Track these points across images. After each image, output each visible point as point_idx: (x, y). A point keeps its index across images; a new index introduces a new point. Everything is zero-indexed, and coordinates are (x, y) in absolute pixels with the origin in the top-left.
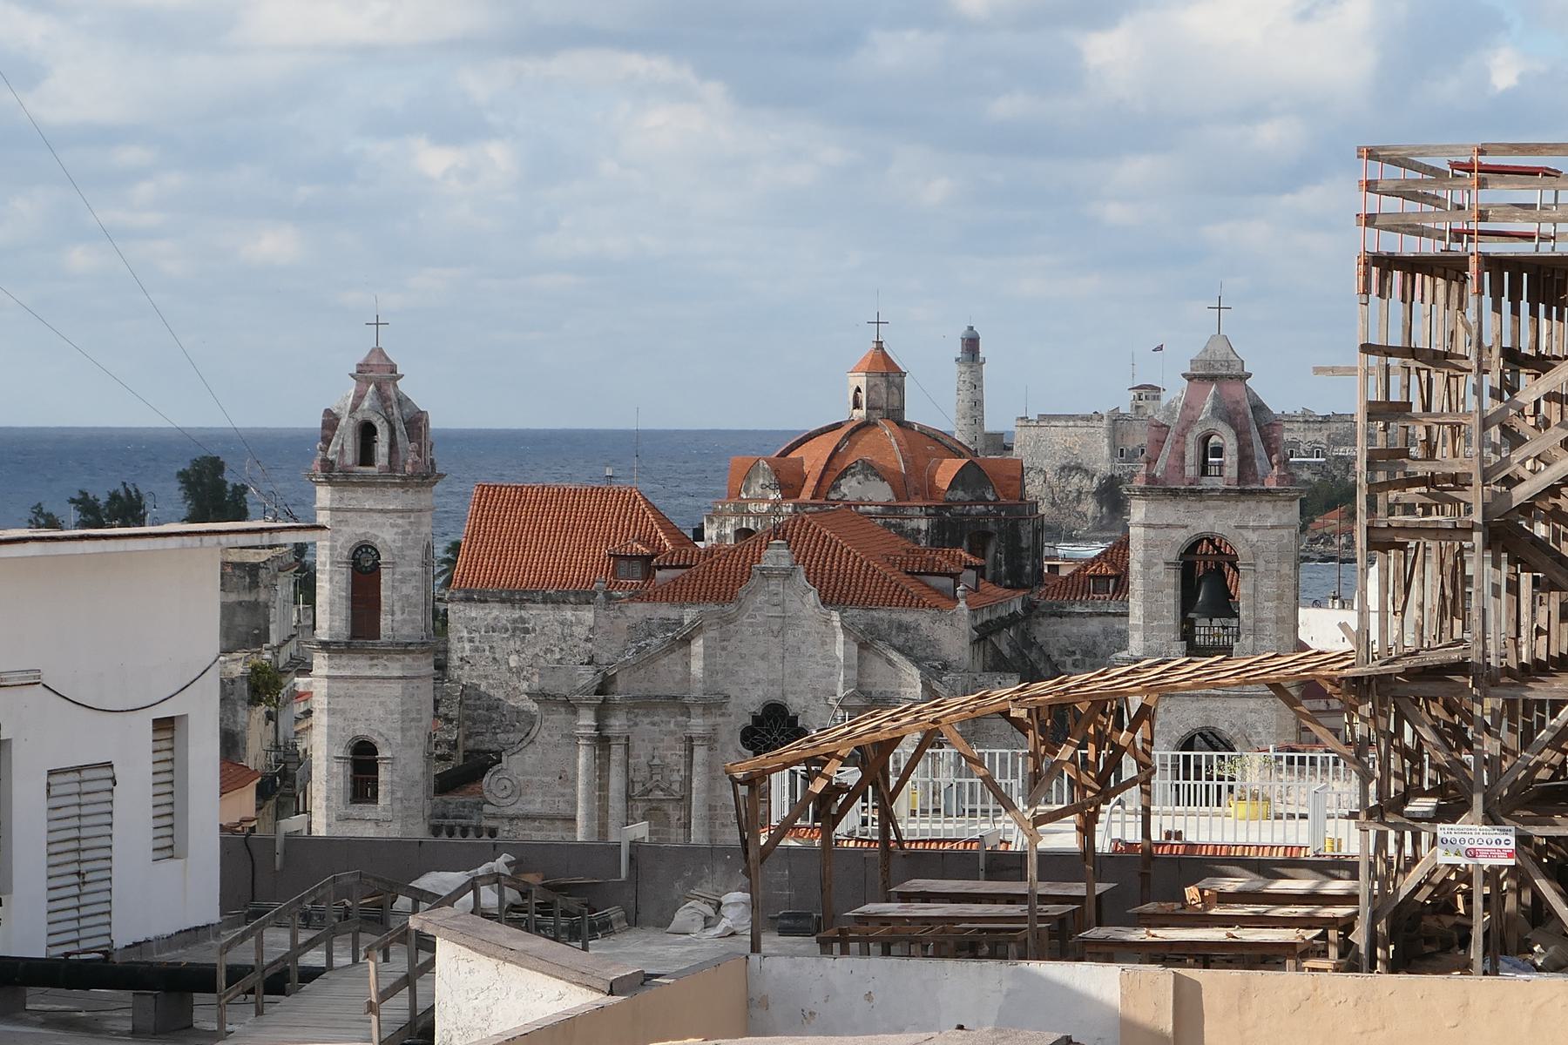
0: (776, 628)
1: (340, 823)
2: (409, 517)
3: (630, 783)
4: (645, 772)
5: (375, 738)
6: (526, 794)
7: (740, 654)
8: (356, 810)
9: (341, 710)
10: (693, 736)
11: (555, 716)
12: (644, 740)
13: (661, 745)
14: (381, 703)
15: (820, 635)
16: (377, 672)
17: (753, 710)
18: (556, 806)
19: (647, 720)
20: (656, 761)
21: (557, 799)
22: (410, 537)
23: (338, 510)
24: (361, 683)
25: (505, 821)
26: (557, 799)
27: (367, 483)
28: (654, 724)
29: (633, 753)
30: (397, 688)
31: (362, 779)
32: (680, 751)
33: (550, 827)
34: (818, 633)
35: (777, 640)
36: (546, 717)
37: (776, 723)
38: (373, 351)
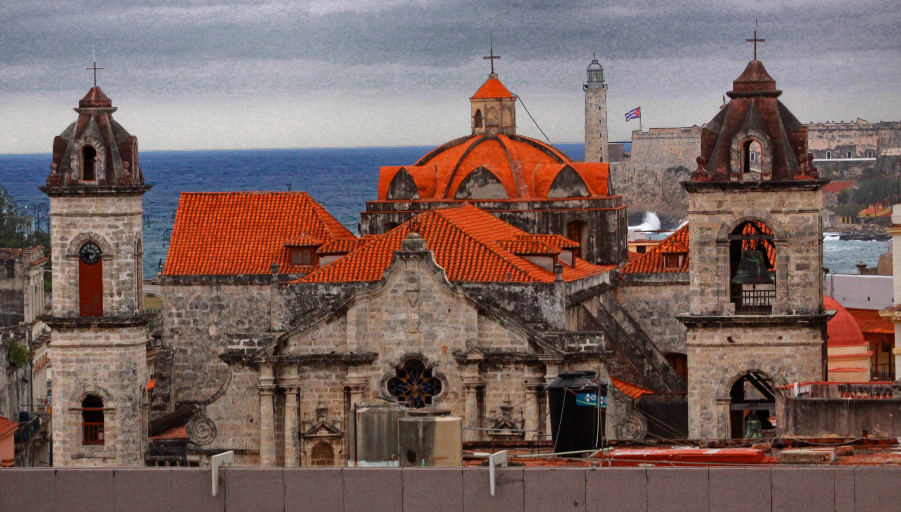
0: (413, 300)
1: (75, 461)
2: (123, 220)
3: (301, 424)
4: (312, 416)
5: (101, 393)
8: (85, 450)
9: (73, 372)
10: (350, 386)
11: (242, 373)
12: (311, 390)
13: (326, 393)
14: (106, 367)
16: (102, 341)
19: (312, 375)
20: (322, 406)
21: (245, 439)
22: (124, 236)
23: (68, 215)
24: (89, 350)
25: (204, 457)
26: (245, 439)
27: (90, 192)
28: (319, 377)
29: (304, 400)
30: (115, 352)
31: (91, 426)
32: (340, 397)
33: (239, 460)
34: (446, 303)
35: (414, 309)
36: (235, 374)
37: (415, 373)
38: (92, 90)
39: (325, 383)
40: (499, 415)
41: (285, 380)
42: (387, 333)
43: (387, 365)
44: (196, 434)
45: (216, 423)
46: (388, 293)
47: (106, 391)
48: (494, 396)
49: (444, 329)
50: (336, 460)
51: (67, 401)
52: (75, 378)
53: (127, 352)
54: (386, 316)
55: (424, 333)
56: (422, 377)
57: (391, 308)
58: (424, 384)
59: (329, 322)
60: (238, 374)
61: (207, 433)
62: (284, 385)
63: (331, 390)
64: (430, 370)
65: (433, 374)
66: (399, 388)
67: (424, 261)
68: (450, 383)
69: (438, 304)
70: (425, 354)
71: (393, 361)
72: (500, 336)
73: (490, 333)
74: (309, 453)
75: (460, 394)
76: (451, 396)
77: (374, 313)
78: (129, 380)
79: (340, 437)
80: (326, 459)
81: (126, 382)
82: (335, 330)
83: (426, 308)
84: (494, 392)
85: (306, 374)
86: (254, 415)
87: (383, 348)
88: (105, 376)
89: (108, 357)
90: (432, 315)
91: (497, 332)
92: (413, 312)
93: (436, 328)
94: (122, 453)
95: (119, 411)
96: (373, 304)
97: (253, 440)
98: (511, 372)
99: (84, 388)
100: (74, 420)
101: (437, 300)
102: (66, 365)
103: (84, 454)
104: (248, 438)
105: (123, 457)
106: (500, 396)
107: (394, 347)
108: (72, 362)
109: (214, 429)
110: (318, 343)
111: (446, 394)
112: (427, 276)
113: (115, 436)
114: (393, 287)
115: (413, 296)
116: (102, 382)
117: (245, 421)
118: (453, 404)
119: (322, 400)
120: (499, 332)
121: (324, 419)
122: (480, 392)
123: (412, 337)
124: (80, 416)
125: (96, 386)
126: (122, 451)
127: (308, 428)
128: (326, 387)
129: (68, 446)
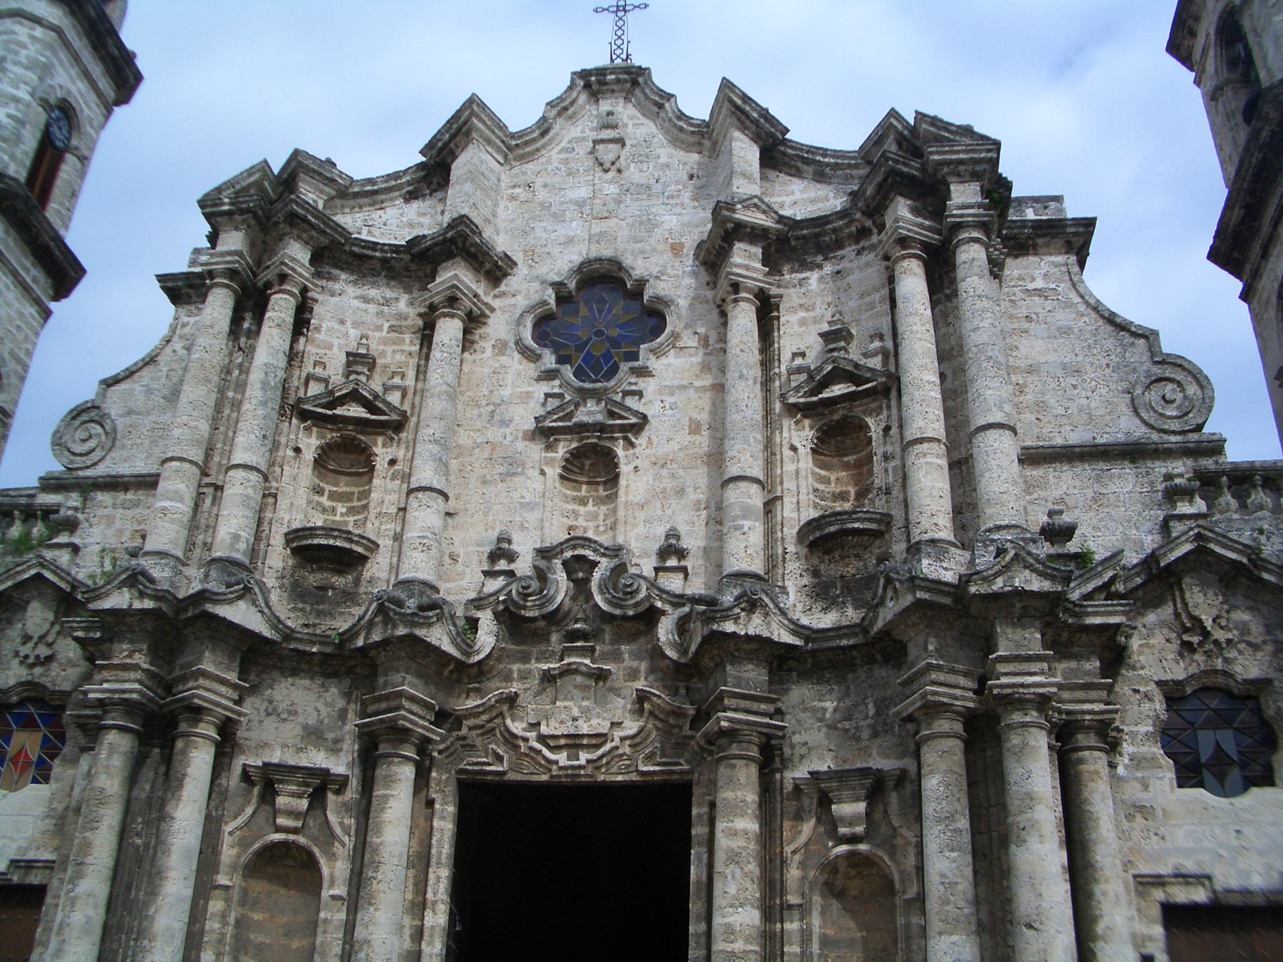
7: (541, 204)
10: (436, 300)
12: (342, 322)
13: (377, 334)
15: (688, 167)
17: (557, 279)
19: (351, 291)
20: (362, 351)
28: (366, 300)
32: (411, 344)
34: (685, 164)
35: (612, 174)
36: (186, 319)
39: (380, 314)
42: (544, 224)
43: (536, 285)
44: (70, 445)
45: (120, 423)
46: (553, 156)
48: (803, 323)
49: (678, 210)
50: (376, 481)
54: (542, 195)
55: (630, 220)
58: (621, 326)
59: (412, 196)
60: (192, 320)
61: (92, 444)
63: (392, 329)
64: (637, 292)
65: (646, 298)
67: (637, 91)
70: (628, 261)
72: (812, 201)
73: (788, 200)
74: (309, 455)
79: (398, 426)
80: (356, 490)
82: (425, 214)
83: (634, 174)
84: (802, 314)
85: (337, 287)
87: (530, 253)
90: (649, 187)
91: (805, 196)
92: (606, 182)
96: (516, 176)
98: (845, 264)
101: (664, 159)
106: (816, 321)
109: (112, 435)
110: (377, 232)
111: (676, 336)
112: (644, 120)
114: (564, 144)
115: (607, 153)
118: (693, 359)
120: (812, 195)
123: (597, 227)
127: (315, 389)
128: (380, 321)
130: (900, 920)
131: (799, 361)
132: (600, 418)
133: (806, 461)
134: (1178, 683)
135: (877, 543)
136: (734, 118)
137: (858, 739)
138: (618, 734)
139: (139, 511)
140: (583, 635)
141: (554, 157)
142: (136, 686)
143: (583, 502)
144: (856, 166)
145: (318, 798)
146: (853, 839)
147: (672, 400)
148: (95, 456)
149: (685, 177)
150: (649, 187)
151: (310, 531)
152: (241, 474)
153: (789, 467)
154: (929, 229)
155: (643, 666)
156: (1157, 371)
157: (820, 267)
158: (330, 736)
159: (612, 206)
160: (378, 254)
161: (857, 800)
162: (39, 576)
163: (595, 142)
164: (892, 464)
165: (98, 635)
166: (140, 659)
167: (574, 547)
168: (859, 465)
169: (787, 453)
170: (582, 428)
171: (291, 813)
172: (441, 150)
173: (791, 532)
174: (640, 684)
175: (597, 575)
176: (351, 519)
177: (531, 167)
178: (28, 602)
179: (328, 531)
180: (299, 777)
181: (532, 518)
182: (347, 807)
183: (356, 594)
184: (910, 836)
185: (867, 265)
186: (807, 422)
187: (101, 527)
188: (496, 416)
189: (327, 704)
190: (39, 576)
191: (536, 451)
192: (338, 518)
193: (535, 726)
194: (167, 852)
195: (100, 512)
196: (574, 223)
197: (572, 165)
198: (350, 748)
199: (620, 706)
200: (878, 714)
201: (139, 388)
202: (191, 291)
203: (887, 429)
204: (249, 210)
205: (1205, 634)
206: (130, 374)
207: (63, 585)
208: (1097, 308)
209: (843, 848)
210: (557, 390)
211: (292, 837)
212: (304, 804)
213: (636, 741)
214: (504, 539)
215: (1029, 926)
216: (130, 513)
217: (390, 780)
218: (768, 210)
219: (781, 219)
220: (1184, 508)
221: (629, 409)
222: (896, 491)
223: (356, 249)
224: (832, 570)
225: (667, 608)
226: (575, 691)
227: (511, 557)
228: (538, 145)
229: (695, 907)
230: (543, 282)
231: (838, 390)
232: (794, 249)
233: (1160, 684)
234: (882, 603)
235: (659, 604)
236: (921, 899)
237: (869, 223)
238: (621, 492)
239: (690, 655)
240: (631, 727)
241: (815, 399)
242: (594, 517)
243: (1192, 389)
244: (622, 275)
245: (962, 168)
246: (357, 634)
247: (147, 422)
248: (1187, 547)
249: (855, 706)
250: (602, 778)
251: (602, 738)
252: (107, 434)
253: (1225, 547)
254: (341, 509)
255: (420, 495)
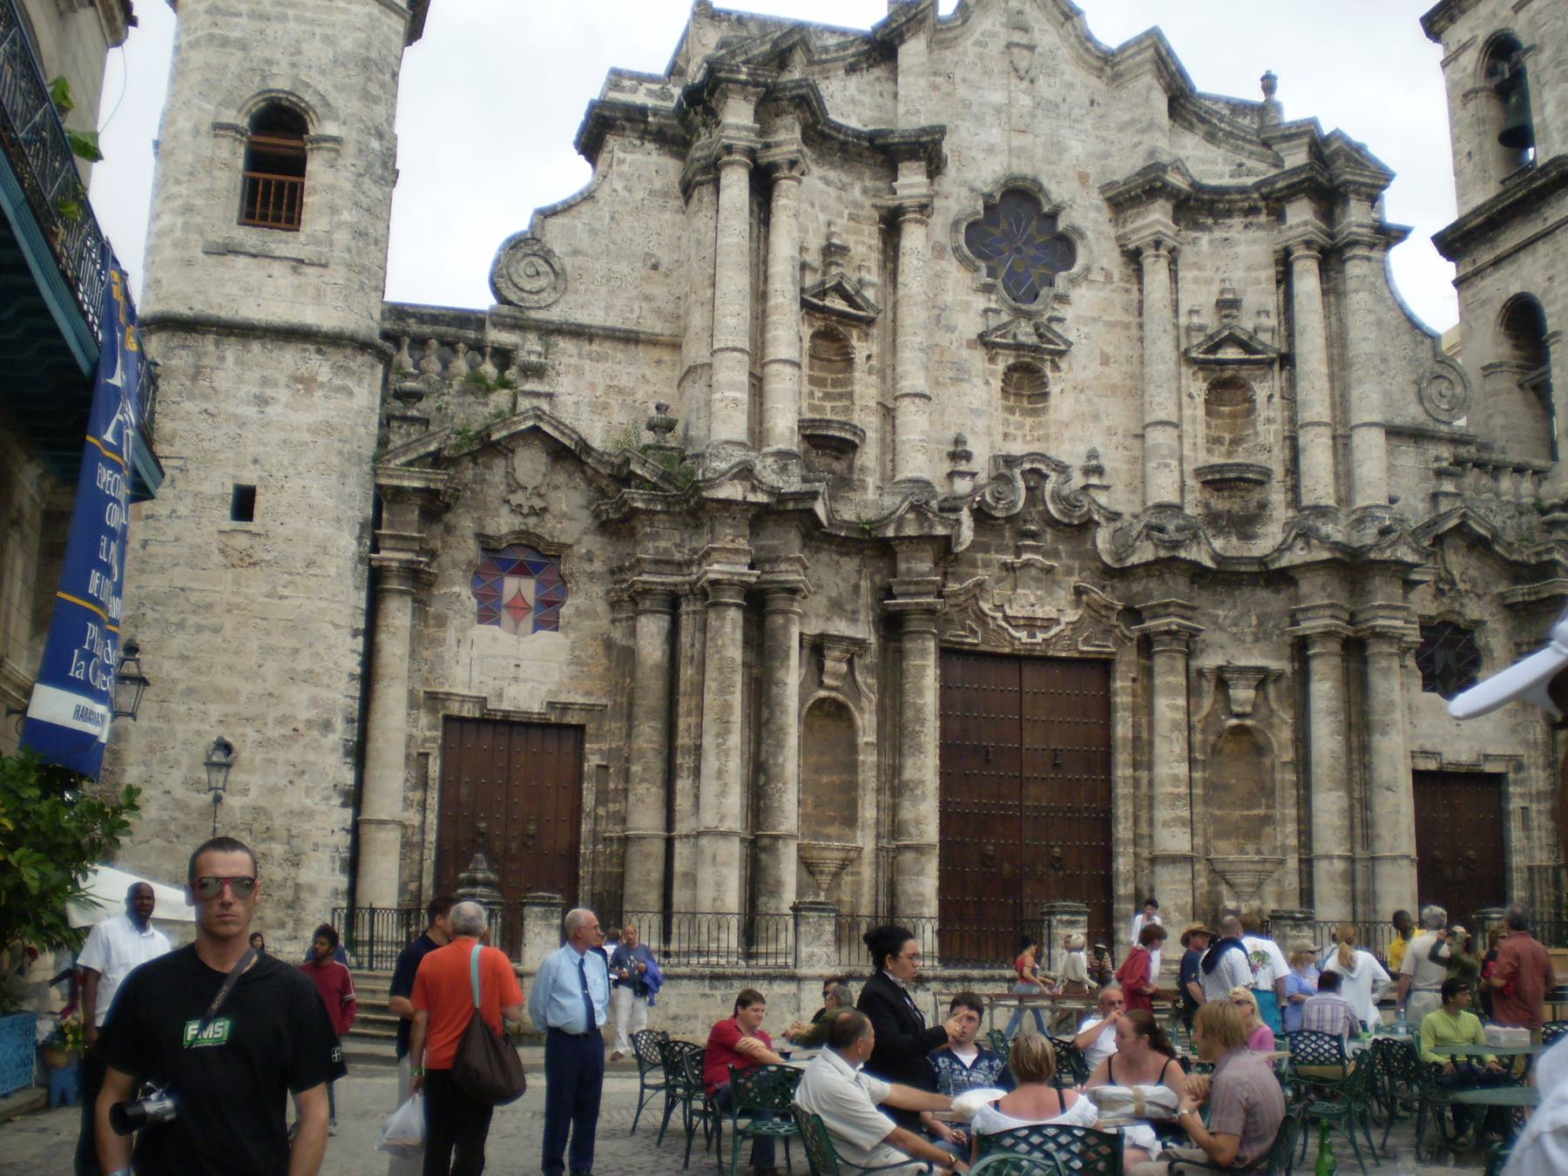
4: (814, 258)
5: (310, 98)
6: (576, 292)
7: (963, 101)
8: (251, 237)
10: (907, 203)
12: (812, 205)
14: (328, 40)
17: (986, 190)
18: (635, 316)
19: (816, 171)
20: (835, 241)
28: (828, 183)
31: (267, 183)
33: (620, 356)
35: (1025, 84)
40: (1209, 320)
41: (778, 145)
42: (967, 124)
43: (965, 192)
44: (515, 277)
45: (569, 263)
47: (323, 98)
50: (857, 374)
51: (210, 107)
52: (240, 54)
53: (384, 19)
56: (1032, 230)
57: (974, 76)
58: (1038, 247)
59: (851, 69)
60: (629, 157)
61: (542, 282)
62: (779, 155)
64: (1053, 217)
65: (1061, 225)
66: (984, 245)
68: (1095, 248)
69: (1070, 86)
70: (1045, 181)
71: (978, 185)
75: (1116, 277)
76: (1096, 275)
77: (939, 80)
78: (383, 86)
79: (870, 322)
80: (830, 376)
81: (374, 89)
82: (862, 92)
83: (1045, 87)
84: (1195, 273)
86: (666, 260)
88: (324, 60)
89: (338, 18)
93: (1065, 132)
94: (346, 255)
95: (350, 150)
97: (657, 311)
99: (264, 79)
100: (224, 153)
101: (1068, 77)
102: (219, 19)
103: (241, 244)
104: (645, 305)
105: (349, 266)
106: (1209, 282)
107: (980, 156)
108: (238, 15)
111: (1088, 269)
112: (1048, 27)
113: (334, 210)
114: (977, 36)
116: (314, 73)
117: (639, 265)
118: (1101, 294)
119: (833, 229)
121: (840, 270)
122: (1173, 262)
123: (1018, 141)
124: (242, 150)
125: (297, 80)
126: (349, 250)
127: (811, 280)
129: (198, 220)
130: (1278, 776)
131: (1196, 320)
132: (1034, 340)
133: (1201, 411)
134: (1431, 618)
135: (1258, 489)
136: (1154, 68)
137: (1243, 642)
138: (1064, 620)
139: (608, 365)
140: (1033, 535)
141: (970, 48)
142: (745, 569)
143: (1011, 411)
144: (1251, 142)
145: (850, 662)
146: (1238, 716)
147: (1084, 330)
148: (547, 297)
149: (1088, 103)
150: (1056, 105)
151: (828, 423)
152: (789, 370)
153: (1187, 412)
154: (1322, 232)
155: (1077, 565)
156: (1438, 369)
157: (1209, 229)
158: (849, 607)
159: (1028, 120)
160: (841, 137)
161: (1249, 687)
162: (535, 430)
163: (1009, 46)
164: (1273, 427)
165: (659, 508)
166: (742, 543)
167: (1032, 462)
168: (1233, 416)
169: (1185, 399)
170: (1018, 347)
171: (836, 675)
172: (893, 31)
173: (1189, 468)
174: (1074, 580)
175: (1049, 486)
176: (828, 405)
177: (948, 54)
178: (513, 451)
179: (843, 425)
180: (844, 645)
181: (981, 424)
182: (869, 669)
183: (851, 480)
184: (1287, 715)
185: (1254, 241)
186: (1200, 375)
187: (571, 377)
188: (939, 318)
189: (843, 580)
190: (535, 430)
191: (977, 358)
192: (816, 402)
193: (1000, 608)
194: (784, 712)
195: (565, 360)
196: (994, 130)
197: (987, 62)
198: (866, 616)
199: (1064, 596)
200: (1260, 624)
201: (580, 226)
202: (628, 125)
203: (1270, 397)
204: (765, 85)
205: (1453, 583)
206: (567, 207)
207: (567, 442)
208: (1401, 307)
209: (1233, 722)
210: (993, 305)
211: (833, 694)
212: (844, 667)
213: (1075, 626)
214: (959, 441)
215: (1389, 789)
216: (601, 366)
217: (923, 653)
218: (1184, 173)
219: (1194, 184)
220: (1448, 486)
221: (1060, 337)
222: (1276, 451)
223: (826, 129)
224: (1220, 504)
225: (1102, 521)
226: (1031, 582)
227: (967, 456)
228: (957, 32)
229: (1122, 757)
230: (972, 190)
231: (1231, 353)
232: (1191, 209)
233: (1420, 616)
234: (1290, 548)
235: (1096, 517)
236: (1303, 764)
237: (1261, 204)
238: (1051, 410)
239: (1129, 563)
240: (1071, 615)
241: (1211, 357)
242: (1021, 426)
243: (1459, 390)
244: (1041, 197)
245: (1363, 189)
246: (887, 526)
247: (600, 266)
248: (1453, 522)
249: (1241, 616)
250: (1050, 653)
251: (1049, 622)
252: (556, 274)
253: (1479, 524)
254: (818, 394)
255: (917, 400)
